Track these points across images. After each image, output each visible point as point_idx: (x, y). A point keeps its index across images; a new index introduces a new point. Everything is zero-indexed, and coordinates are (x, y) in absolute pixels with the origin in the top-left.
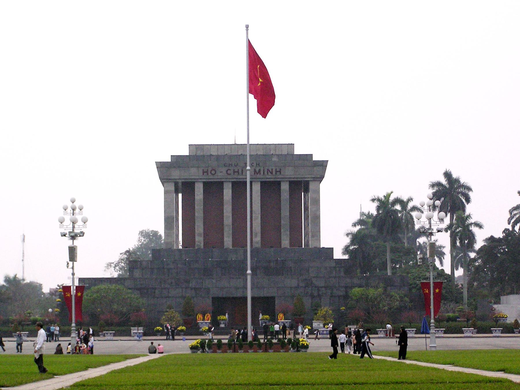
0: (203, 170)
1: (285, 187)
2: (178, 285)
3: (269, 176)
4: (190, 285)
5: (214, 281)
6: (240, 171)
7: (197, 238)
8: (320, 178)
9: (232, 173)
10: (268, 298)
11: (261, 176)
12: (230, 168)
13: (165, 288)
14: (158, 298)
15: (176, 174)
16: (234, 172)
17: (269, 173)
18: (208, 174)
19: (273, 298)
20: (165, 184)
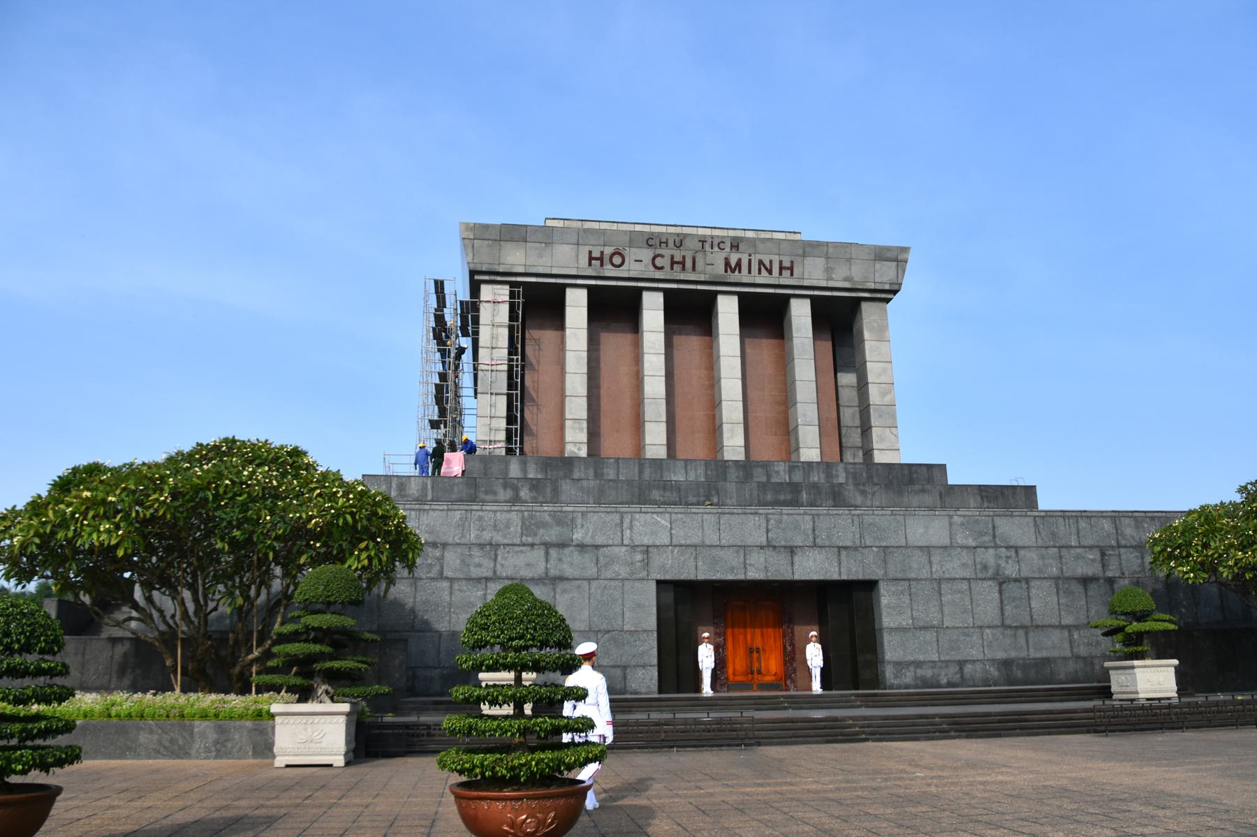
0: (590, 252)
1: (801, 313)
3: (764, 278)
5: (664, 521)
6: (689, 264)
7: (569, 437)
8: (885, 294)
9: (668, 267)
12: (659, 251)
13: (481, 546)
14: (451, 580)
15: (515, 259)
16: (673, 263)
18: (602, 265)
19: (869, 586)
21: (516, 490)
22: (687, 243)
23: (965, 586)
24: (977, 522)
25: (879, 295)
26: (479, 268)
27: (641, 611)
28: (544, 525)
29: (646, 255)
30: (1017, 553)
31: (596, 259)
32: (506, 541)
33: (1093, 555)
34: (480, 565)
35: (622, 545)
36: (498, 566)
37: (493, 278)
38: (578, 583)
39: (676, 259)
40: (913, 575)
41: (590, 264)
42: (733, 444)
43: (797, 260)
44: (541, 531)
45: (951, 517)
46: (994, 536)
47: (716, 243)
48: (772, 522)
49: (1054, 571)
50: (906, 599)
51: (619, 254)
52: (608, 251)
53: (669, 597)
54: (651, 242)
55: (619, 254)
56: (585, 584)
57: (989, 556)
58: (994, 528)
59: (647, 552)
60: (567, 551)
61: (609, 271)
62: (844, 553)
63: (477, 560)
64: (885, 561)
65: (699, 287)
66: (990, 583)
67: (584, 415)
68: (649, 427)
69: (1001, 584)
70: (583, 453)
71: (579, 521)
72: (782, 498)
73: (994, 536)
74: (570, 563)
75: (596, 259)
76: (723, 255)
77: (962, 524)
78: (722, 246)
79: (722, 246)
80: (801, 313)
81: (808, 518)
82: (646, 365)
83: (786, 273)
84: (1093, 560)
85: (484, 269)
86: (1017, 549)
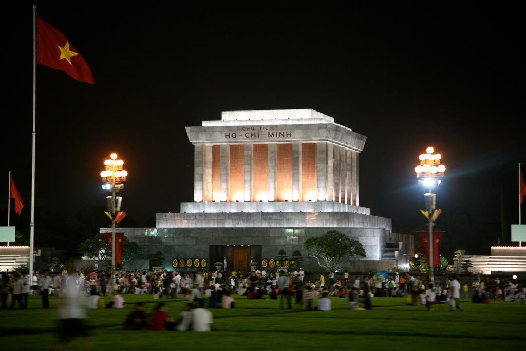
4: (191, 235)
6: (257, 135)
9: (250, 137)
12: (247, 132)
16: (252, 135)
17: (281, 136)
29: (243, 133)
43: (292, 131)
52: (231, 133)
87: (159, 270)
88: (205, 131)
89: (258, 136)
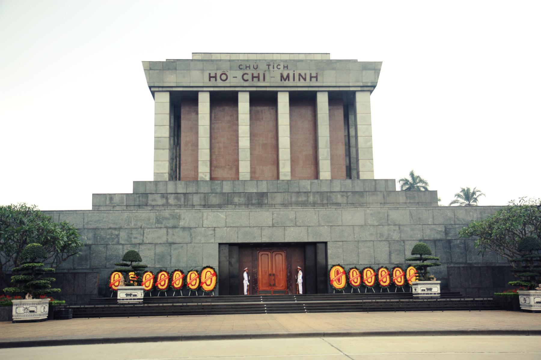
0: (210, 74)
1: (323, 100)
2: (162, 223)
3: (302, 83)
6: (261, 77)
8: (371, 88)
9: (250, 79)
10: (314, 244)
11: (291, 83)
14: (123, 245)
15: (172, 80)
16: (253, 77)
18: (216, 80)
20: (156, 94)
21: (167, 199)
22: (260, 67)
23: (371, 244)
24: (379, 213)
25: (365, 89)
26: (152, 85)
27: (212, 257)
28: (167, 219)
29: (239, 74)
30: (400, 228)
31: (213, 77)
32: (148, 227)
33: (441, 228)
34: (136, 238)
35: (203, 227)
36: (145, 238)
37: (161, 89)
38: (182, 245)
39: (254, 75)
40: (345, 239)
41: (210, 80)
42: (285, 169)
44: (165, 222)
45: (365, 211)
46: (388, 220)
47: (275, 66)
48: (275, 215)
49: (419, 237)
50: (340, 250)
51: (225, 74)
52: (219, 73)
53: (226, 250)
54: (241, 67)
55: (225, 74)
56: (185, 246)
57: (385, 230)
58: (388, 216)
59: (214, 230)
60: (177, 230)
61: (220, 83)
62: (310, 229)
63: (135, 236)
64: (331, 233)
65: (268, 89)
66: (384, 243)
67: (208, 158)
68: (241, 163)
69: (390, 244)
70: (208, 178)
71: (182, 217)
72: (300, 199)
73: (388, 220)
74: (178, 236)
75: (213, 77)
76: (280, 71)
77: (371, 214)
78: (279, 67)
79: (279, 67)
80: (323, 100)
81: (292, 212)
82: (240, 132)
83: (314, 80)
84: (441, 231)
85: (156, 85)
86: (399, 225)
87: (134, 292)
88: (176, 69)
89: (264, 80)
